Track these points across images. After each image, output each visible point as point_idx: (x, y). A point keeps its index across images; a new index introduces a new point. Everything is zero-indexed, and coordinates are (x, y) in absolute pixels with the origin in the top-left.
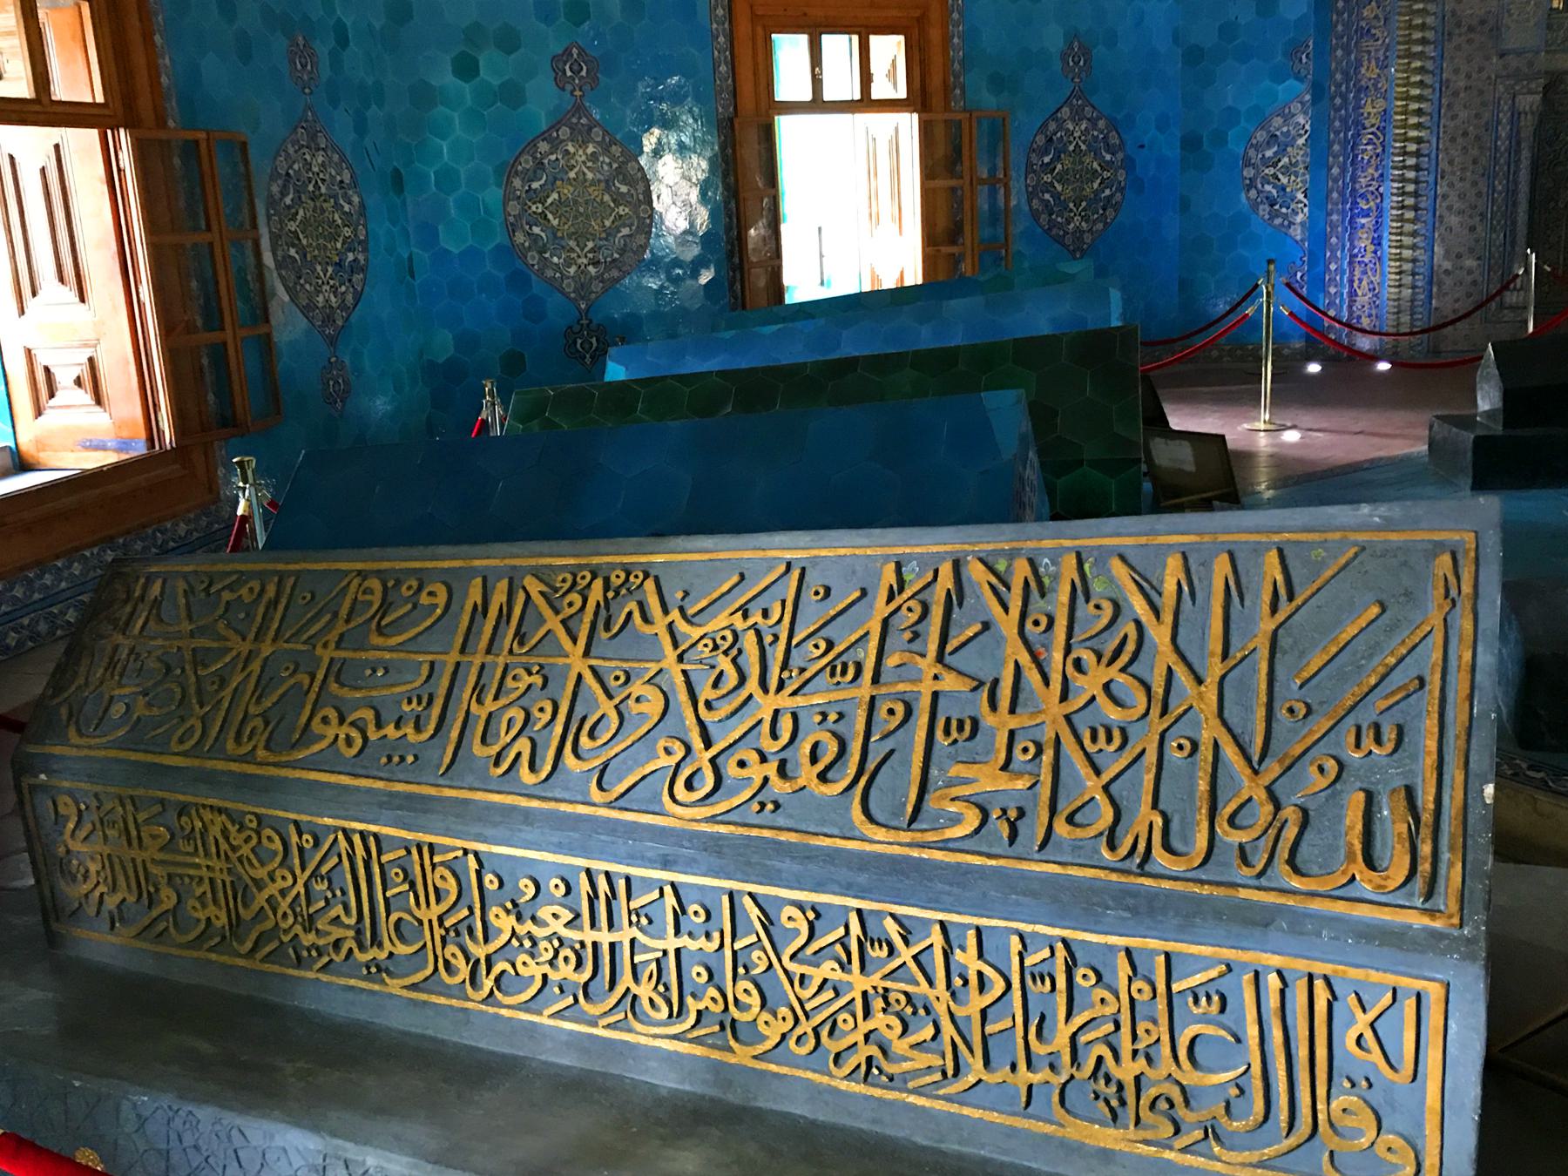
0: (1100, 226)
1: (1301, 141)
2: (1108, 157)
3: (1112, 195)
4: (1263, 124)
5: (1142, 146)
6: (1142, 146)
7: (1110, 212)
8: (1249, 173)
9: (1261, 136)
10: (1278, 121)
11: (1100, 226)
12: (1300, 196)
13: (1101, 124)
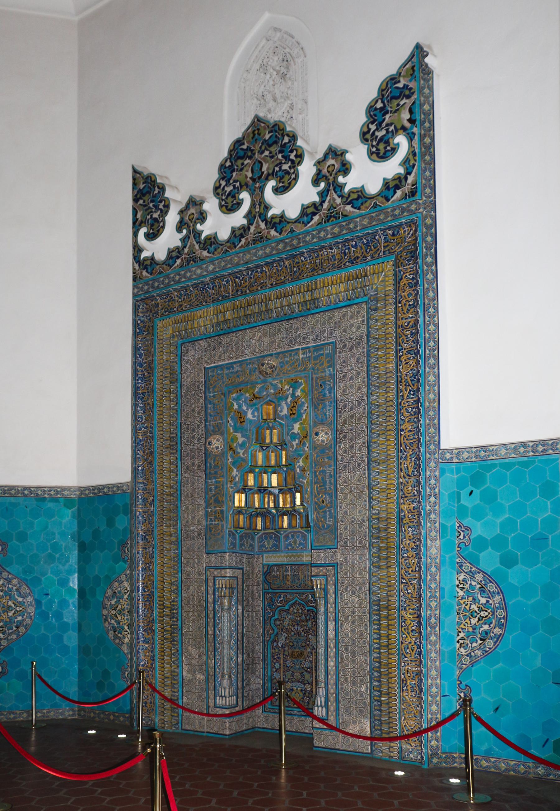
0: (14, 636)
1: (126, 597)
2: (20, 599)
3: (23, 620)
4: (111, 586)
5: (47, 594)
6: (47, 594)
7: (22, 630)
8: (105, 612)
9: (110, 592)
10: (116, 584)
11: (14, 636)
12: (126, 628)
13: (15, 581)
